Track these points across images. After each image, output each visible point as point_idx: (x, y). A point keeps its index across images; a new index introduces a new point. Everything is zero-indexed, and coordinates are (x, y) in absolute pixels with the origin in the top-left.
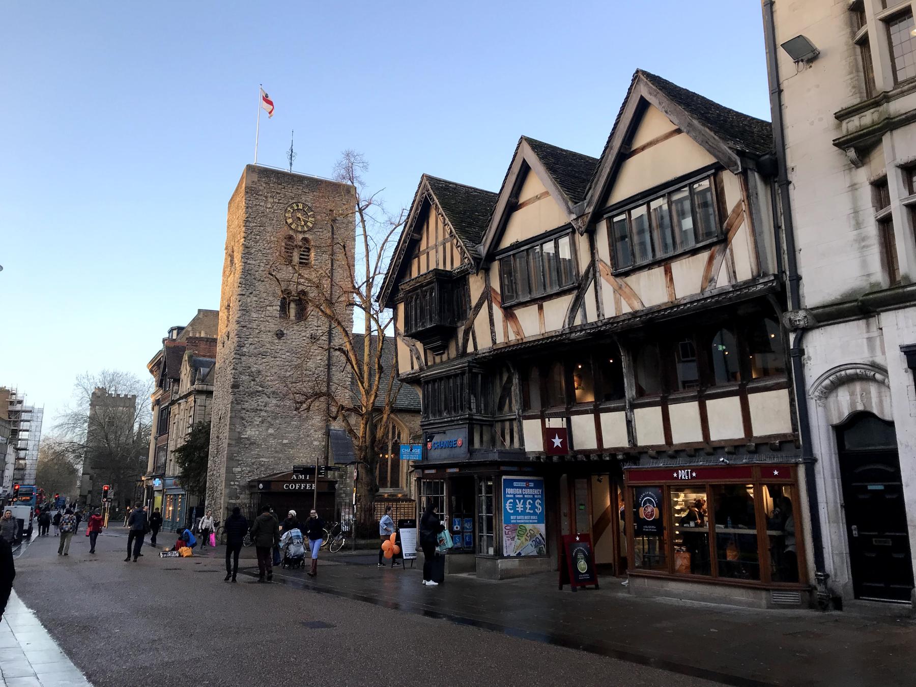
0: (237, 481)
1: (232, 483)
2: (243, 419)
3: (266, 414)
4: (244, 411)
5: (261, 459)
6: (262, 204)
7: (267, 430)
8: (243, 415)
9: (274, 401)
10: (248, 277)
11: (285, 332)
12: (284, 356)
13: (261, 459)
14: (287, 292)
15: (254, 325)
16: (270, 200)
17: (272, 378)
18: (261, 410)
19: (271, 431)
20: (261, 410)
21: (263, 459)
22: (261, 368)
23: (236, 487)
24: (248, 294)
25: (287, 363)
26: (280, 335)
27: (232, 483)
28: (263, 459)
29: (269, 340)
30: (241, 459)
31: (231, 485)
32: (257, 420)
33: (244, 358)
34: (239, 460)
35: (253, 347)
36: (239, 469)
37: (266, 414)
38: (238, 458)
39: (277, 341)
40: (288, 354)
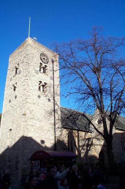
0: (26, 157)
1: (24, 157)
2: (27, 129)
3: (35, 128)
4: (28, 125)
5: (34, 147)
6: (33, 50)
7: (36, 134)
8: (27, 127)
9: (38, 122)
10: (29, 74)
11: (41, 96)
12: (40, 105)
13: (34, 147)
14: (41, 82)
15: (31, 91)
16: (36, 50)
17: (37, 113)
18: (34, 126)
19: (37, 135)
20: (34, 126)
21: (35, 147)
22: (34, 109)
23: (25, 159)
24: (29, 79)
25: (41, 108)
26: (39, 97)
27: (24, 157)
28: (35, 147)
29: (36, 98)
30: (27, 146)
31: (23, 158)
32: (33, 130)
33: (27, 103)
34: (26, 147)
35: (30, 100)
36: (26, 151)
37: (35, 128)
38: (26, 146)
39: (38, 99)
40: (41, 104)
